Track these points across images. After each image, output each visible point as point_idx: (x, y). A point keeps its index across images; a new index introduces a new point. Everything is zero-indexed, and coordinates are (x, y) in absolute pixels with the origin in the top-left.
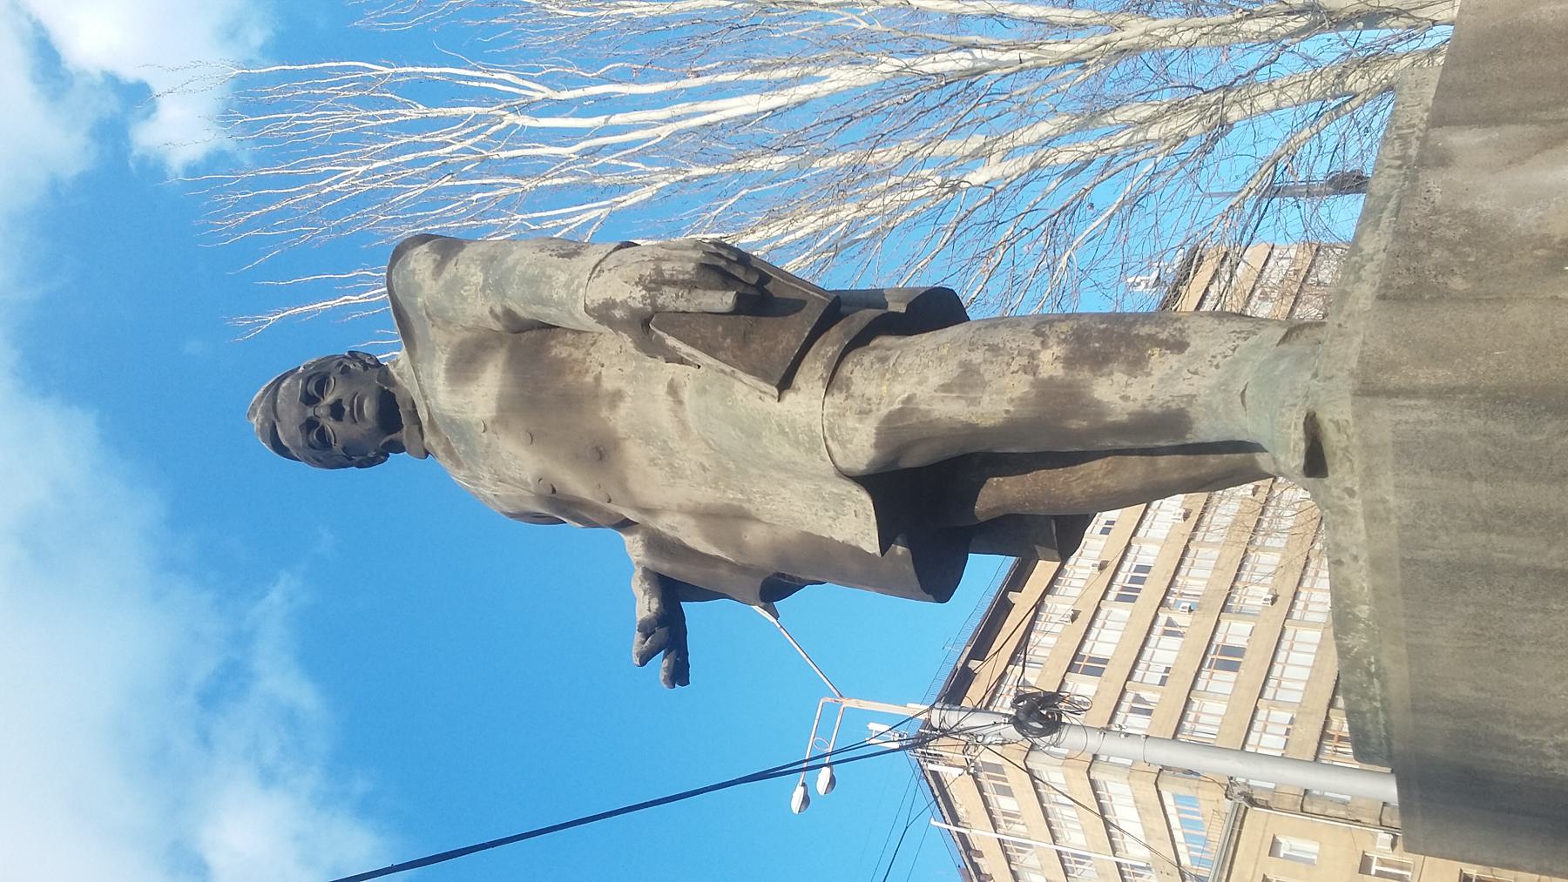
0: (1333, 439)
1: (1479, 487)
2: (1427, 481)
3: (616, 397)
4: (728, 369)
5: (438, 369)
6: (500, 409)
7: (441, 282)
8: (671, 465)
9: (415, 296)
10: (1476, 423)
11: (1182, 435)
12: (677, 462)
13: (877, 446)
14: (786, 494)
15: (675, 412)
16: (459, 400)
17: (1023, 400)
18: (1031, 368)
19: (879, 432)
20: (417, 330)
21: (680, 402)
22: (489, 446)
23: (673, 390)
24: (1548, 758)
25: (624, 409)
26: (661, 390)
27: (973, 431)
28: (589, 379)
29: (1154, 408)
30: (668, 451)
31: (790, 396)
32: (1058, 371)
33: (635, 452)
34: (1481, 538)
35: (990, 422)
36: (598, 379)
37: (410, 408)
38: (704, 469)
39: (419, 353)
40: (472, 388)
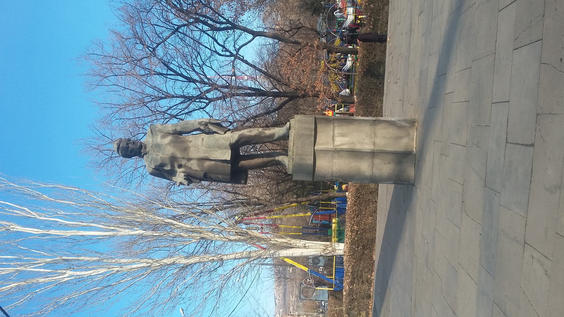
0: (291, 125)
1: (304, 125)
2: (300, 124)
3: (192, 141)
5: (159, 137)
6: (170, 142)
7: (162, 126)
8: (198, 151)
9: (156, 128)
10: (304, 118)
11: (273, 138)
12: (199, 150)
13: (238, 137)
14: (217, 153)
15: (202, 142)
16: (162, 141)
17: (257, 133)
18: (258, 130)
19: (239, 136)
20: (154, 133)
21: (203, 141)
22: (164, 148)
23: (203, 139)
24: (307, 161)
25: (192, 143)
26: (200, 139)
27: (250, 136)
28: (186, 139)
29: (272, 133)
30: (198, 148)
31: (225, 134)
32: (261, 130)
33: (192, 149)
34: (303, 131)
35: (253, 135)
36: (188, 139)
37: (145, 146)
38: (204, 151)
39: (153, 136)
40: (165, 139)
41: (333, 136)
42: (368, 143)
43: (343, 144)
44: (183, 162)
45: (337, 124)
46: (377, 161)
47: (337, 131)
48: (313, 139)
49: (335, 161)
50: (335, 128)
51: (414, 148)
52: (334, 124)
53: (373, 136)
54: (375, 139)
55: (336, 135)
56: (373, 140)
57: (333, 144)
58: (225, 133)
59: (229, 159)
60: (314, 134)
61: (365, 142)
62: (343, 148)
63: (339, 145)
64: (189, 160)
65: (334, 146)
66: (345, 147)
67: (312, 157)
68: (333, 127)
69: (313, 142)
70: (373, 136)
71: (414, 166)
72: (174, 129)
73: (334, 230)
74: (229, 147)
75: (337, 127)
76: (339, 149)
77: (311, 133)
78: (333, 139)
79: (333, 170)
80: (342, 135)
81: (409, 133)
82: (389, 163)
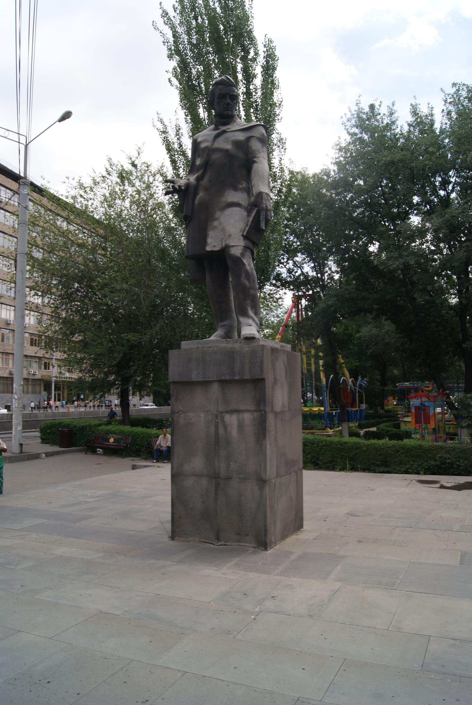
4: (249, 224)
10: (259, 360)
24: (196, 370)
41: (238, 411)
42: (230, 469)
43: (225, 427)
44: (205, 182)
45: (255, 416)
46: (204, 482)
47: (247, 417)
48: (228, 378)
49: (202, 415)
50: (251, 413)
51: (224, 542)
52: (256, 411)
53: (242, 476)
54: (238, 480)
55: (241, 416)
56: (235, 476)
57: (225, 412)
58: (245, 237)
59: (208, 249)
60: (235, 378)
61: (232, 463)
62: (219, 429)
63: (223, 421)
64: (206, 189)
65: (222, 412)
66: (221, 431)
67: (202, 378)
68: (252, 409)
69: (223, 378)
70: (242, 476)
71: (201, 540)
72: (255, 159)
73: (311, 410)
74: (224, 245)
75: (252, 417)
76: (218, 422)
77: (237, 374)
78: (232, 412)
79: (189, 414)
80: (241, 426)
81: (248, 535)
82: (203, 502)
